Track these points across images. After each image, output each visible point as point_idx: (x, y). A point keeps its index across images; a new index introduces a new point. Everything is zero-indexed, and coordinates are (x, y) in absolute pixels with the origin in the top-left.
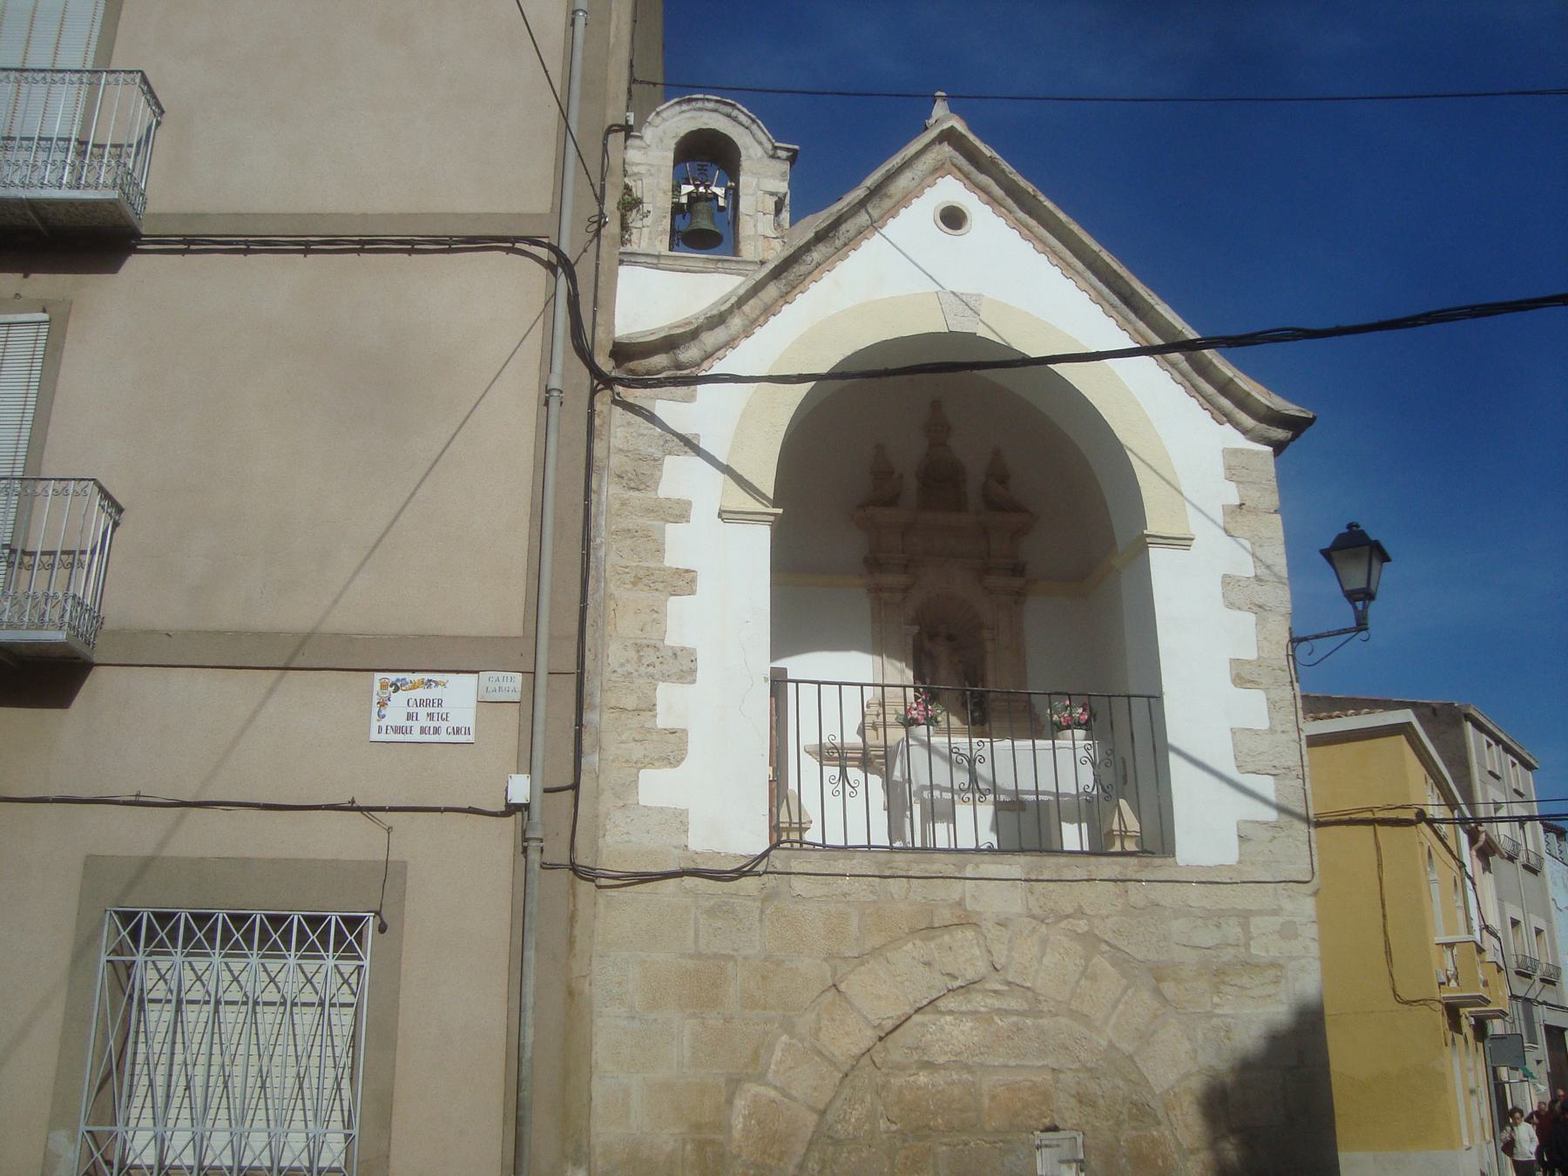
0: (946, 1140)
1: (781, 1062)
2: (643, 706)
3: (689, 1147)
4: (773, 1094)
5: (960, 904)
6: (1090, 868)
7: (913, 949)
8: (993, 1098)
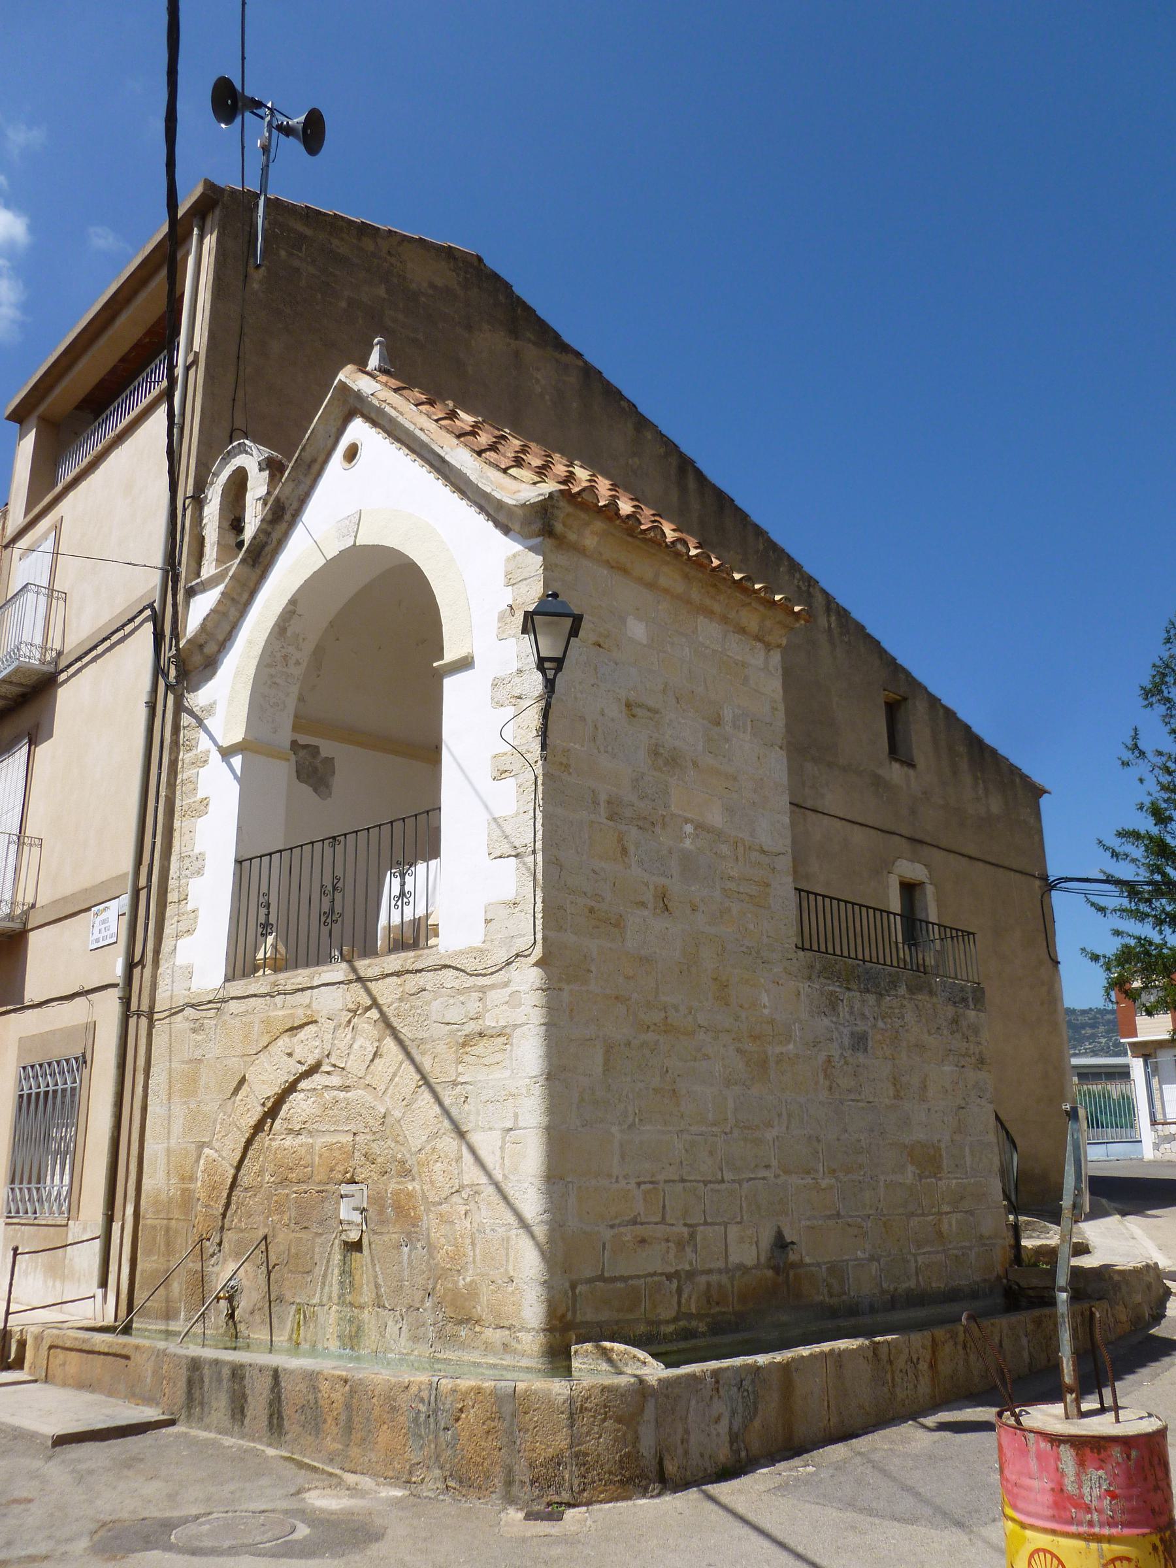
0: (295, 1189)
1: (220, 1132)
2: (182, 898)
3: (178, 1193)
4: (216, 1155)
5: (309, 1006)
6: (384, 965)
7: (284, 1042)
8: (321, 1156)
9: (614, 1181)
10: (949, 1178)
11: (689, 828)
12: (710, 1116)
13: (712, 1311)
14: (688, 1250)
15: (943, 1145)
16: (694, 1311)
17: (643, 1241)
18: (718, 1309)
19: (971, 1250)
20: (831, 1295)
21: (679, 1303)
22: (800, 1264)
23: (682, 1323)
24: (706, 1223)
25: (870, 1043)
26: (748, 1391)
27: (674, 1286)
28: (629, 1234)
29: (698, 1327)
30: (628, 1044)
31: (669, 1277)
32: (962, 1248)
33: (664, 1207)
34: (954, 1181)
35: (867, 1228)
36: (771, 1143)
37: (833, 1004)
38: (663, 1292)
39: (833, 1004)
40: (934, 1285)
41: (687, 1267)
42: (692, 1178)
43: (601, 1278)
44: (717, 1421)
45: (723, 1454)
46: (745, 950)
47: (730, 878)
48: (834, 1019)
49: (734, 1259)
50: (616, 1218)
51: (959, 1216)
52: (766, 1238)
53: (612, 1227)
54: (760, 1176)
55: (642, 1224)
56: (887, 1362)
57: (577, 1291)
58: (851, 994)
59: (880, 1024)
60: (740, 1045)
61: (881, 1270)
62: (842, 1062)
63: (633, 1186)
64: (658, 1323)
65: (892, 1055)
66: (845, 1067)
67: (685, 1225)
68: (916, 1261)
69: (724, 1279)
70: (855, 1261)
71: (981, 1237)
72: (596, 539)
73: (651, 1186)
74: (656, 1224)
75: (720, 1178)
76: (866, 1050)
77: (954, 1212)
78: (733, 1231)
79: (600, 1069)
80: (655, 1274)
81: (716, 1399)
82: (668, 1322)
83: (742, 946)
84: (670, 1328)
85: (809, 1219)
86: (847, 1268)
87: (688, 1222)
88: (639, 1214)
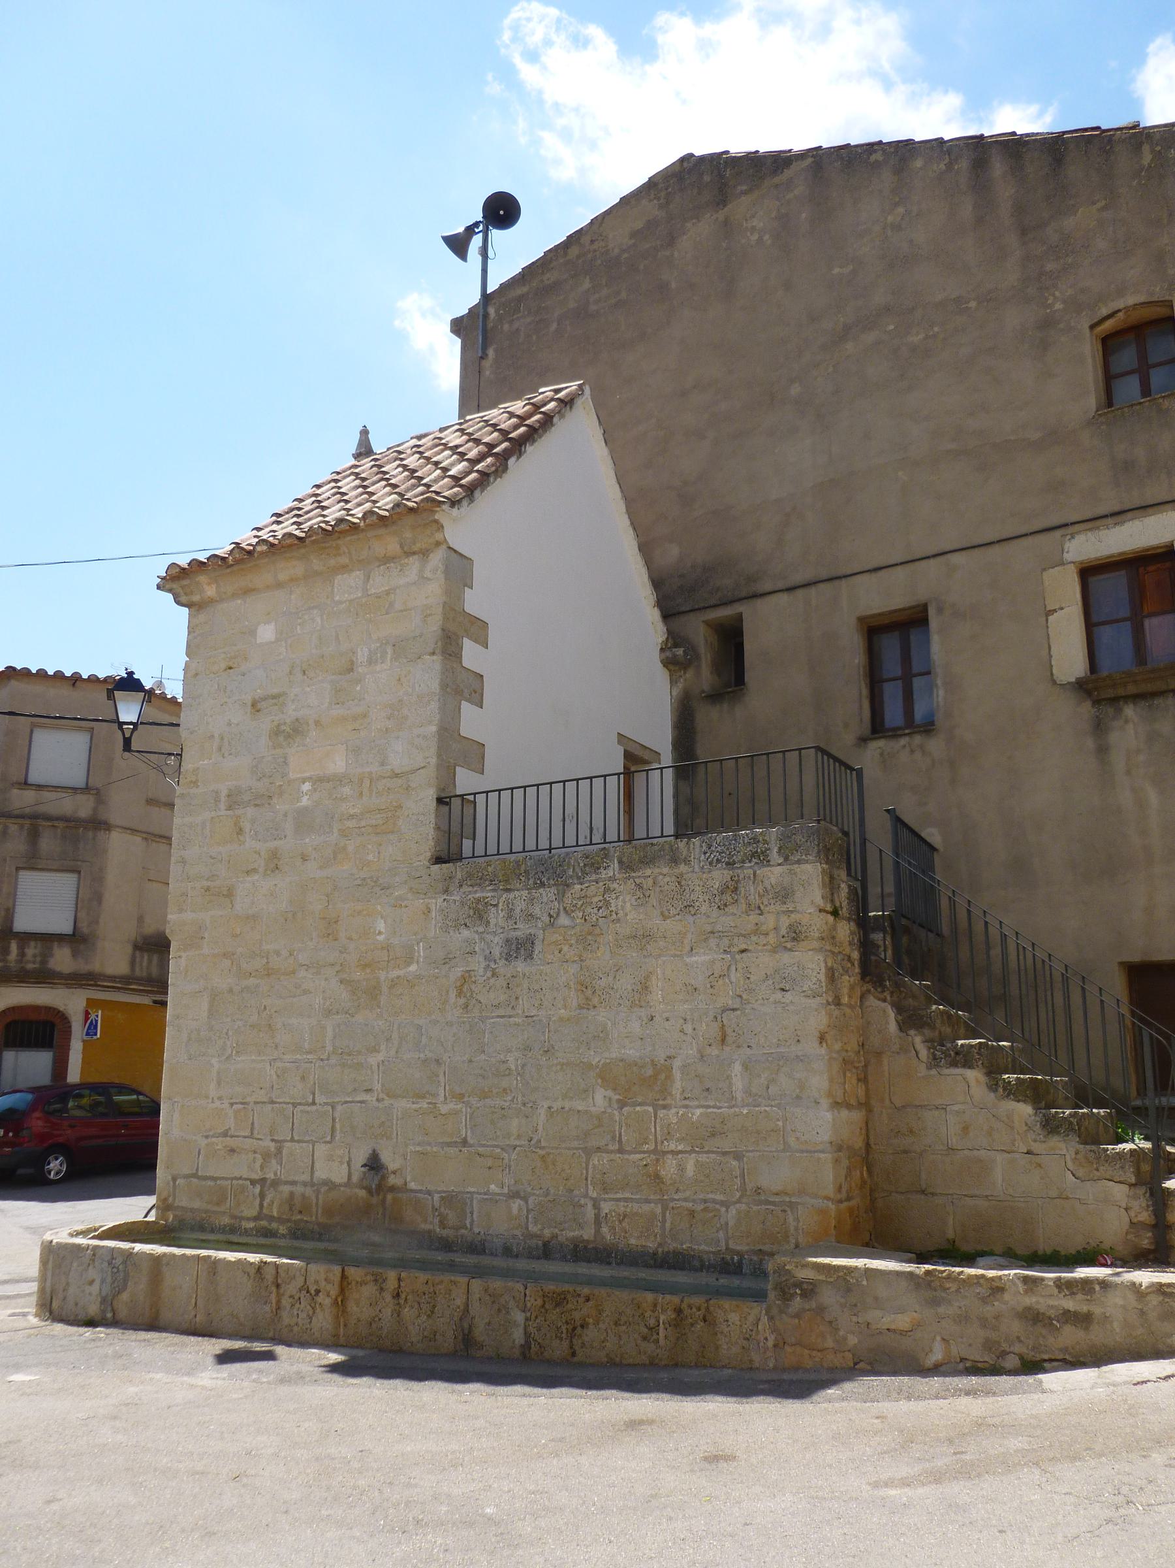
9: (210, 1101)
10: (686, 1107)
11: (307, 787)
12: (306, 1045)
13: (294, 1218)
14: (274, 1161)
15: (677, 1064)
16: (275, 1214)
17: (233, 1151)
18: (299, 1217)
19: (727, 1208)
20: (443, 1225)
21: (261, 1206)
22: (404, 1189)
23: (264, 1223)
24: (292, 1140)
25: (538, 948)
26: (118, 1268)
27: (257, 1189)
28: (220, 1143)
29: (277, 1230)
30: (231, 991)
31: (253, 1182)
32: (705, 1201)
33: (253, 1124)
34: (698, 1112)
35: (510, 1160)
36: (375, 1068)
37: (479, 913)
38: (246, 1194)
39: (479, 913)
40: (633, 1241)
41: (273, 1177)
42: (281, 1100)
43: (195, 1176)
44: (91, 1282)
45: (93, 1310)
46: (360, 883)
47: (351, 817)
48: (481, 929)
49: (321, 1174)
50: (210, 1130)
51: (703, 1158)
52: (361, 1156)
53: (207, 1137)
54: (358, 1099)
55: (232, 1137)
56: (273, 1283)
57: (177, 1183)
58: (512, 895)
59: (564, 920)
60: (345, 976)
61: (528, 1211)
62: (489, 974)
63: (226, 1105)
64: (242, 1218)
65: (581, 956)
66: (492, 981)
67: (273, 1140)
68: (596, 1206)
69: (309, 1191)
70: (485, 1194)
71: (758, 1190)
72: (214, 586)
73: (241, 1106)
74: (245, 1137)
75: (311, 1101)
76: (530, 956)
77: (692, 1151)
78: (321, 1150)
79: (206, 1014)
80: (240, 1178)
81: (91, 1267)
82: (248, 1219)
83: (356, 879)
84: (252, 1225)
85: (419, 1144)
86: (472, 1201)
87: (276, 1138)
88: (230, 1128)
